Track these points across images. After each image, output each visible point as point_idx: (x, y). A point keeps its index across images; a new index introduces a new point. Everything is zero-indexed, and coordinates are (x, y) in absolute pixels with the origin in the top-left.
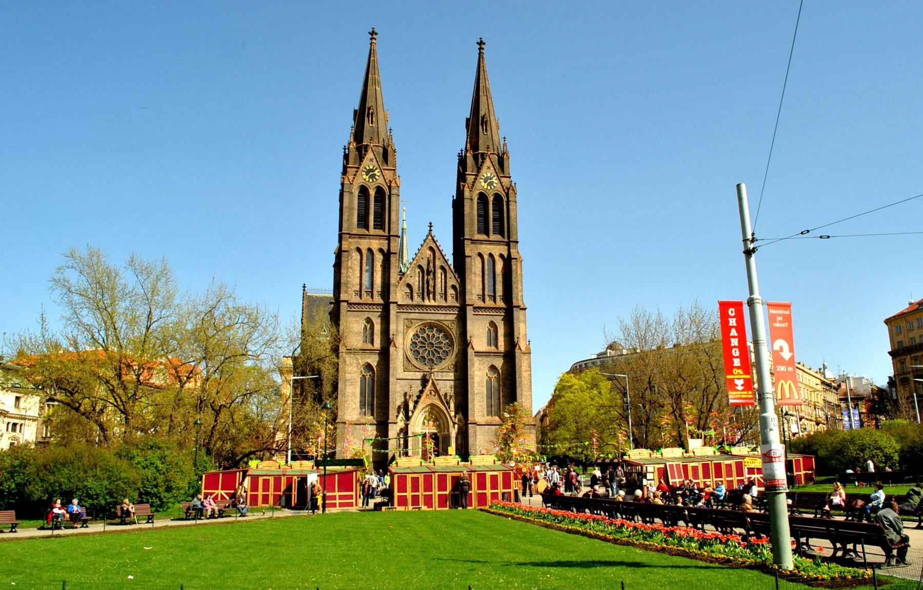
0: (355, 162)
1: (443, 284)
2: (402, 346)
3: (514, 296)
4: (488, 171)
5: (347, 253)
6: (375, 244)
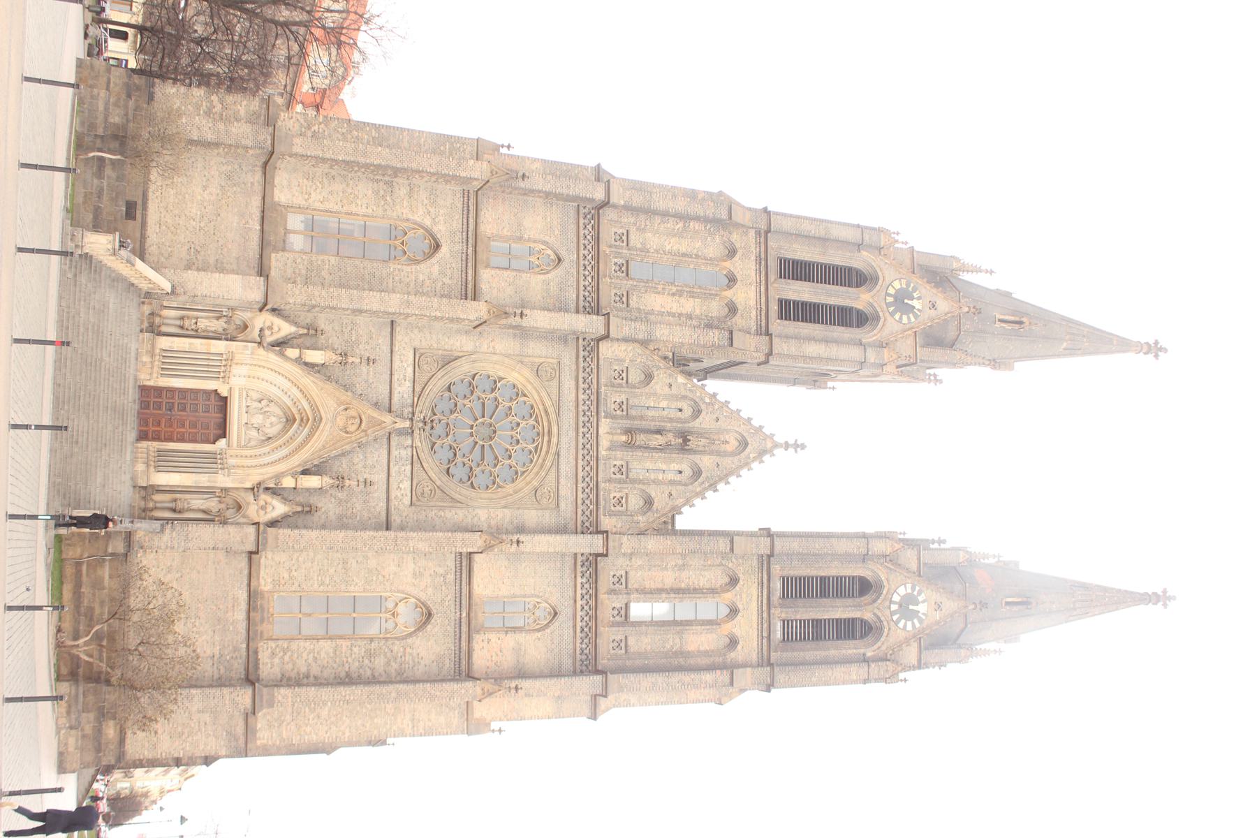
0: (921, 265)
1: (653, 476)
2: (484, 348)
5: (724, 216)
6: (746, 296)
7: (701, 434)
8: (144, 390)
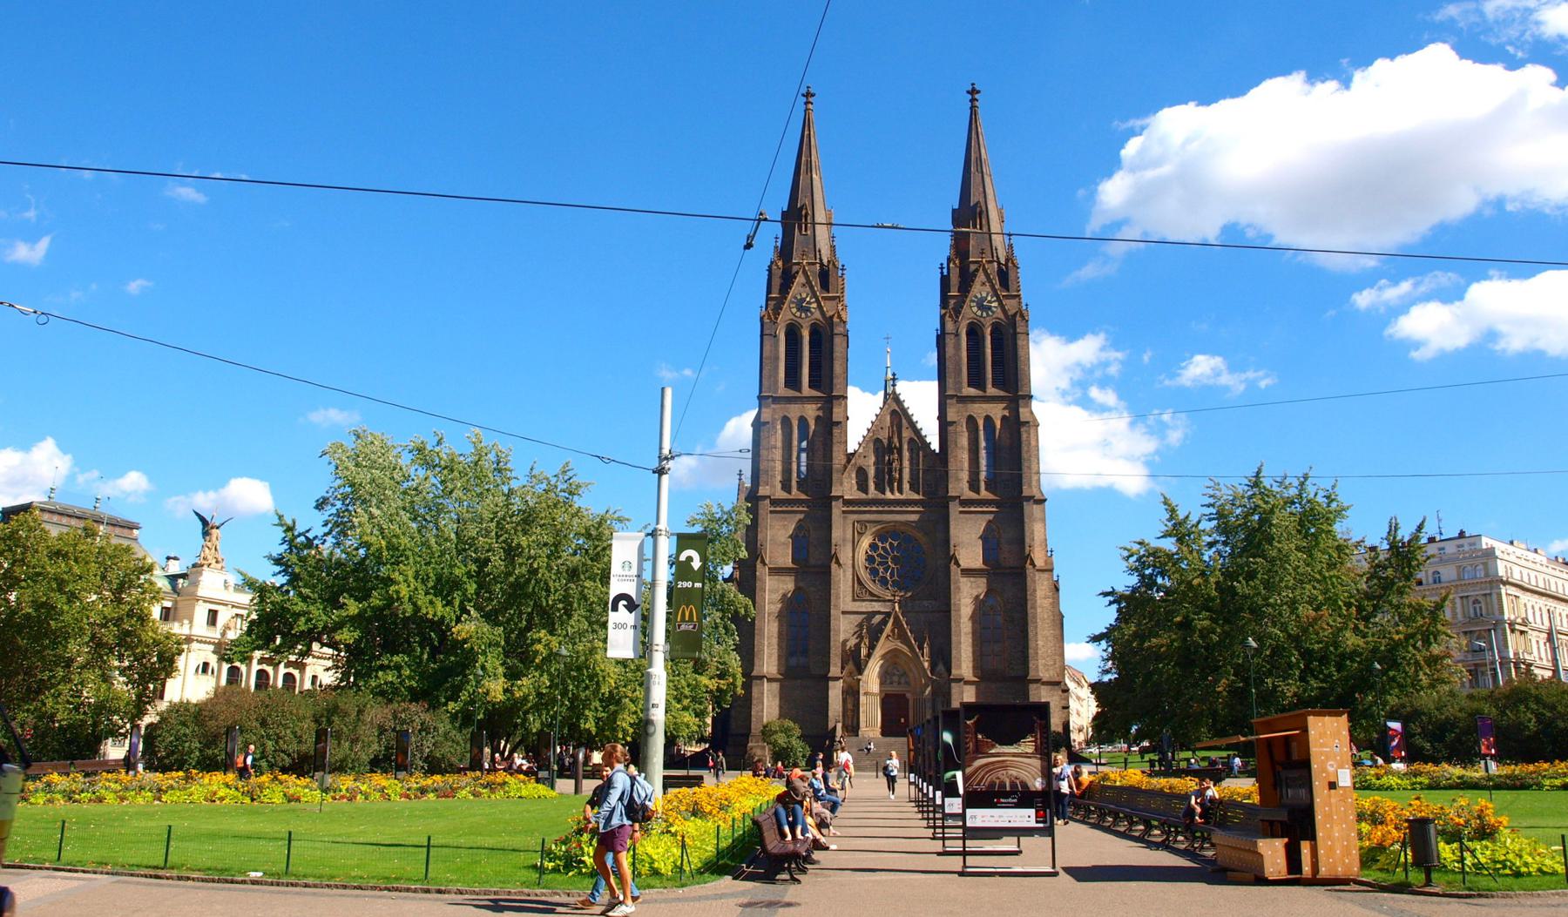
3: (1024, 480)
4: (980, 289)
7: (890, 439)
8: (884, 733)
